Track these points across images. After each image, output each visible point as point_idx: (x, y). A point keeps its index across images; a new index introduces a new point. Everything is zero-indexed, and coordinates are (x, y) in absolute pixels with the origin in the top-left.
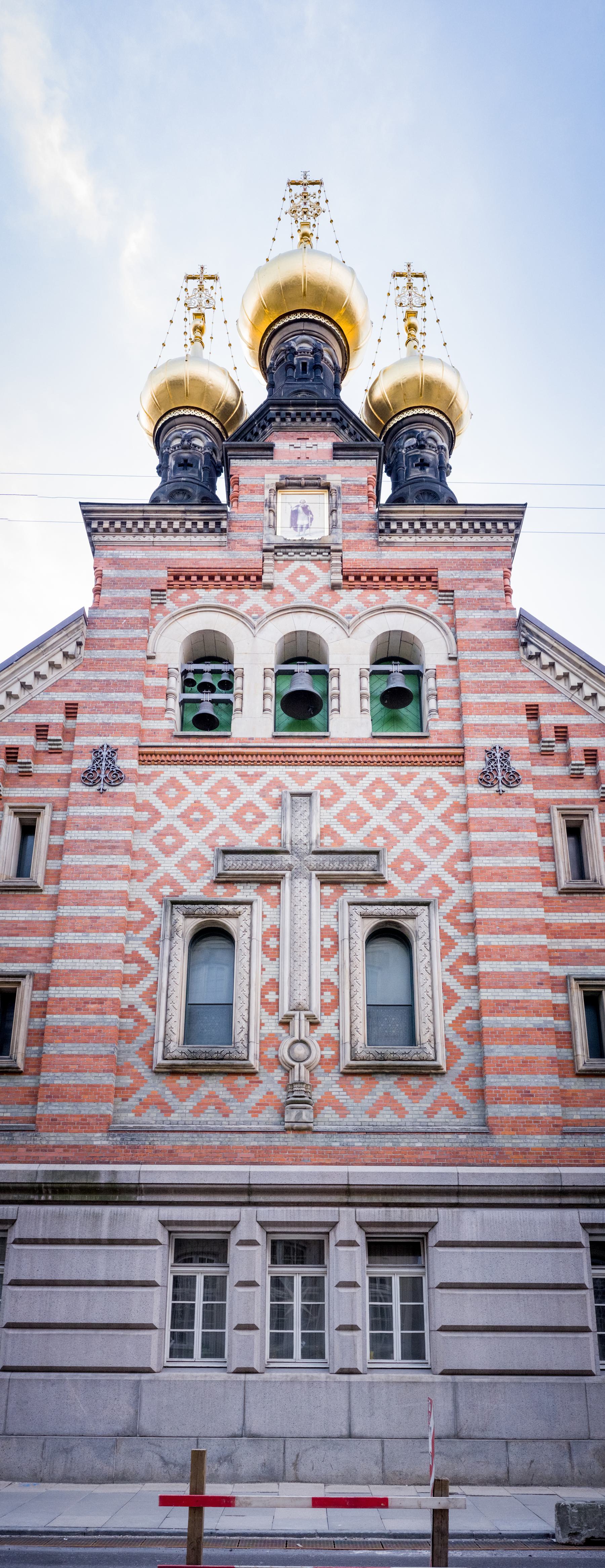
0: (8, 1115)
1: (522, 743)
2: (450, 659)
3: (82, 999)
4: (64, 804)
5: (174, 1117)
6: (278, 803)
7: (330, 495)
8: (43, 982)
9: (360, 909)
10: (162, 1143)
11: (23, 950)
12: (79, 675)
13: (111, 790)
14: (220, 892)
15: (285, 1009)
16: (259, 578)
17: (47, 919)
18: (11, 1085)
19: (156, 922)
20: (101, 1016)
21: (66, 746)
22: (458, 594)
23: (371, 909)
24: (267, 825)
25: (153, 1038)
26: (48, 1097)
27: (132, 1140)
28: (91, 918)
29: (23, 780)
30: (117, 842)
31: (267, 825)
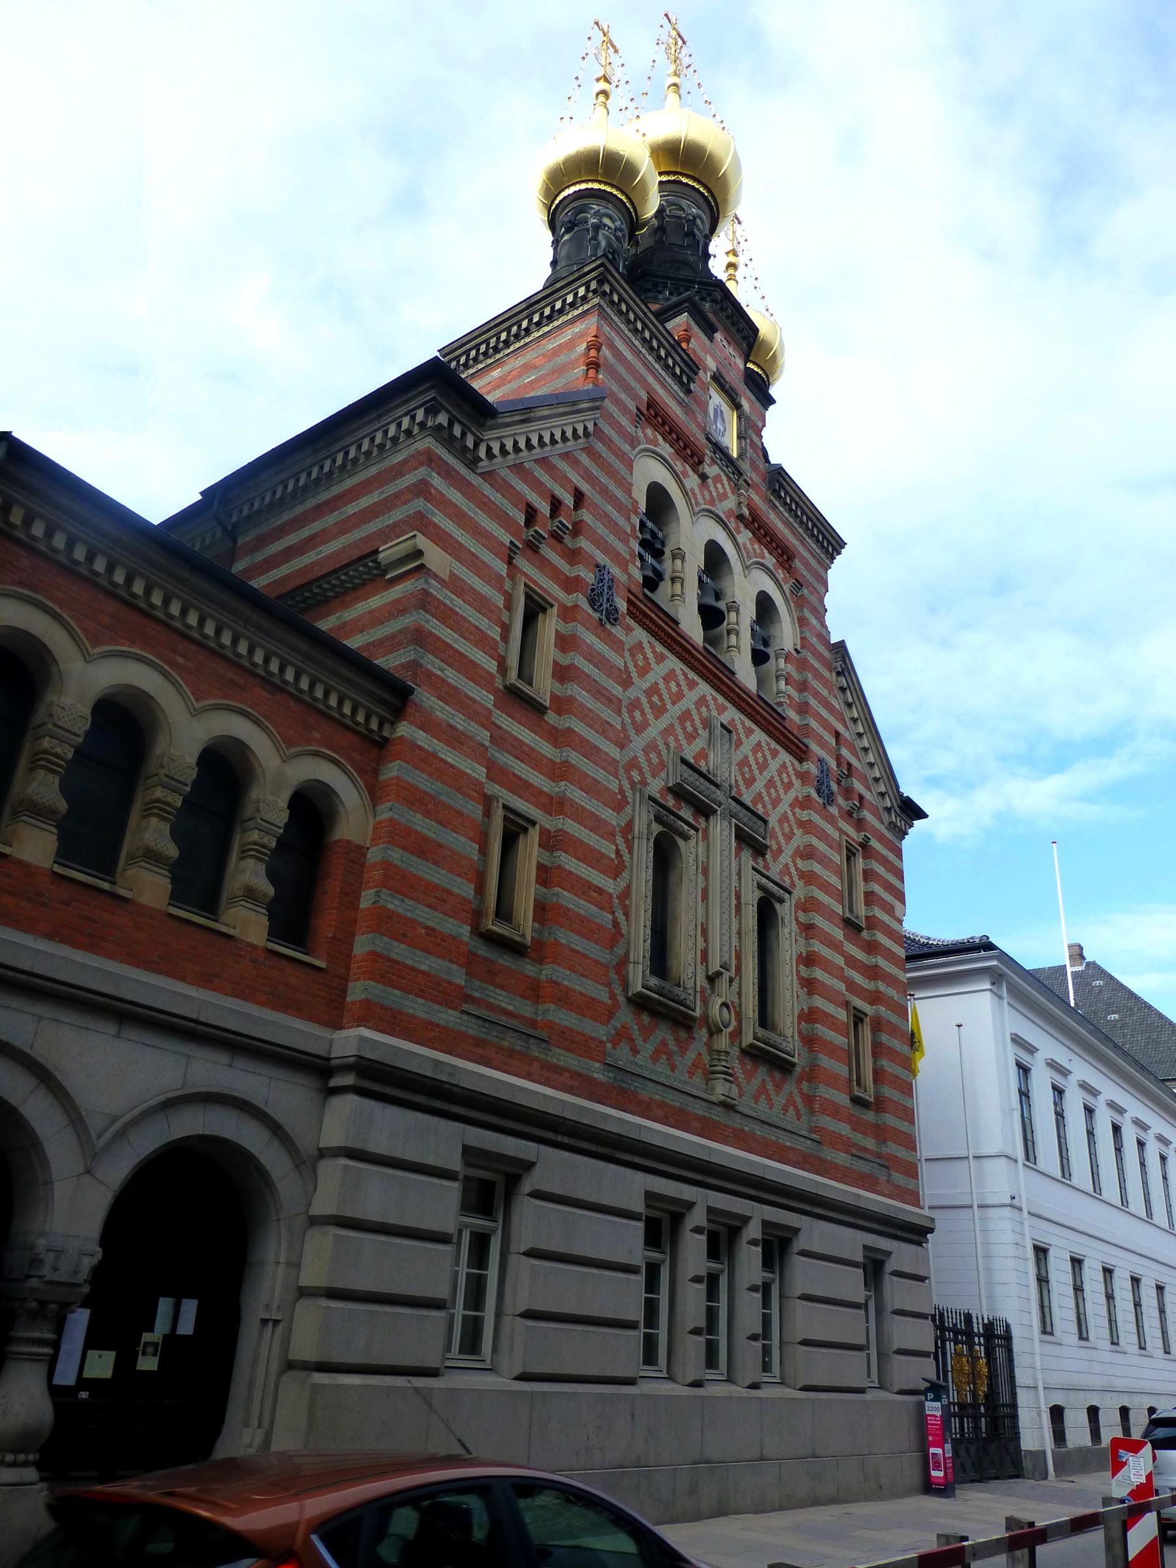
0: (511, 1008)
1: (833, 764)
2: (796, 650)
3: (587, 881)
4: (568, 613)
5: (639, 1059)
6: (707, 724)
7: (739, 418)
8: (550, 842)
9: (758, 877)
10: (648, 1092)
11: (528, 785)
12: (584, 459)
13: (608, 626)
14: (671, 802)
15: (715, 967)
16: (701, 462)
17: (548, 755)
18: (514, 966)
19: (628, 809)
20: (599, 911)
21: (567, 539)
22: (805, 591)
23: (764, 881)
24: (700, 743)
25: (627, 954)
26: (559, 1000)
27: (622, 1081)
28: (594, 779)
29: (529, 552)
30: (613, 695)
31: (700, 743)
